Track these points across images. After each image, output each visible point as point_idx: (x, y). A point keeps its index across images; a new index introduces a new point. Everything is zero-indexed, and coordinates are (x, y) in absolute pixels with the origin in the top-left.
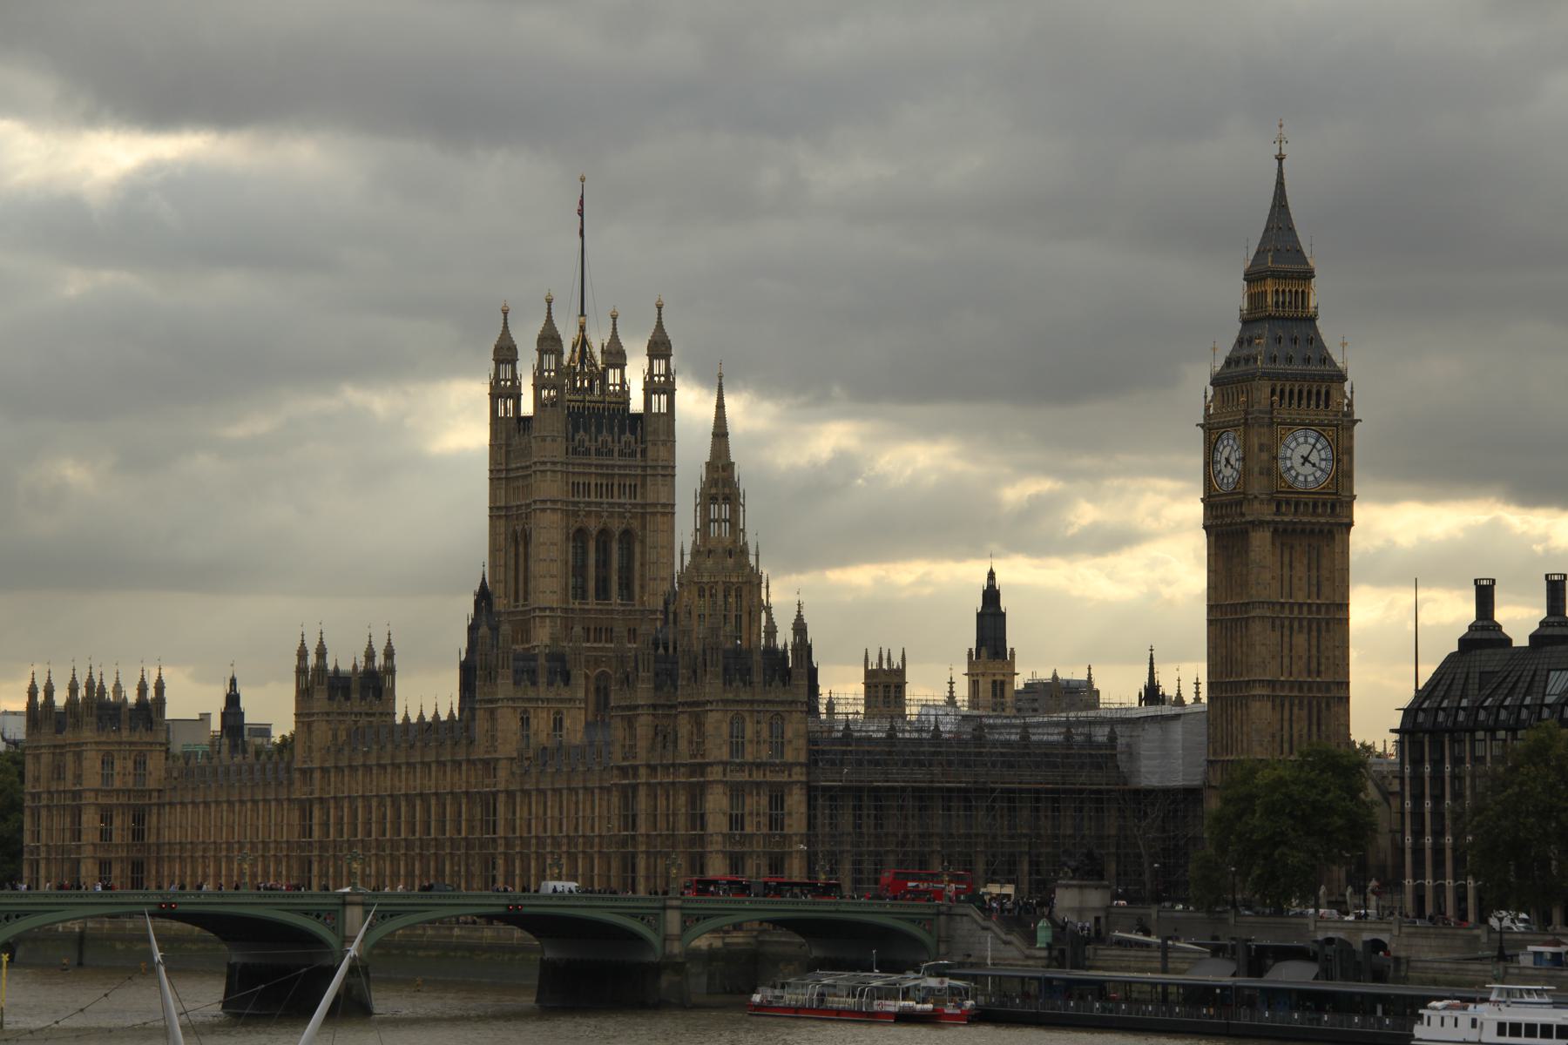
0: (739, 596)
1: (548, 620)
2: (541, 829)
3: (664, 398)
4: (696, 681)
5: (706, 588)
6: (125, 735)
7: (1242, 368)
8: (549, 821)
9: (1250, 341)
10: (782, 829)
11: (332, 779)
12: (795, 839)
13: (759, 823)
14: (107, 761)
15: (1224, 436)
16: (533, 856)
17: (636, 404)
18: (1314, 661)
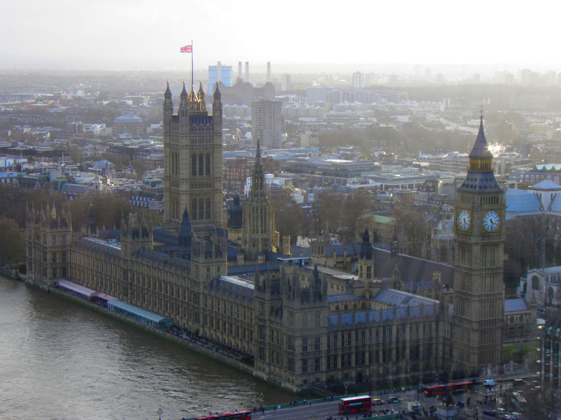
0: (265, 209)
1: (185, 183)
2: (217, 310)
3: (219, 111)
4: (290, 300)
5: (255, 207)
6: (59, 229)
7: (469, 189)
8: (220, 309)
9: (472, 180)
10: (319, 349)
11: (135, 266)
12: (324, 352)
13: (312, 348)
14: (54, 237)
15: (463, 211)
16: (214, 318)
17: (210, 114)
18: (492, 286)
